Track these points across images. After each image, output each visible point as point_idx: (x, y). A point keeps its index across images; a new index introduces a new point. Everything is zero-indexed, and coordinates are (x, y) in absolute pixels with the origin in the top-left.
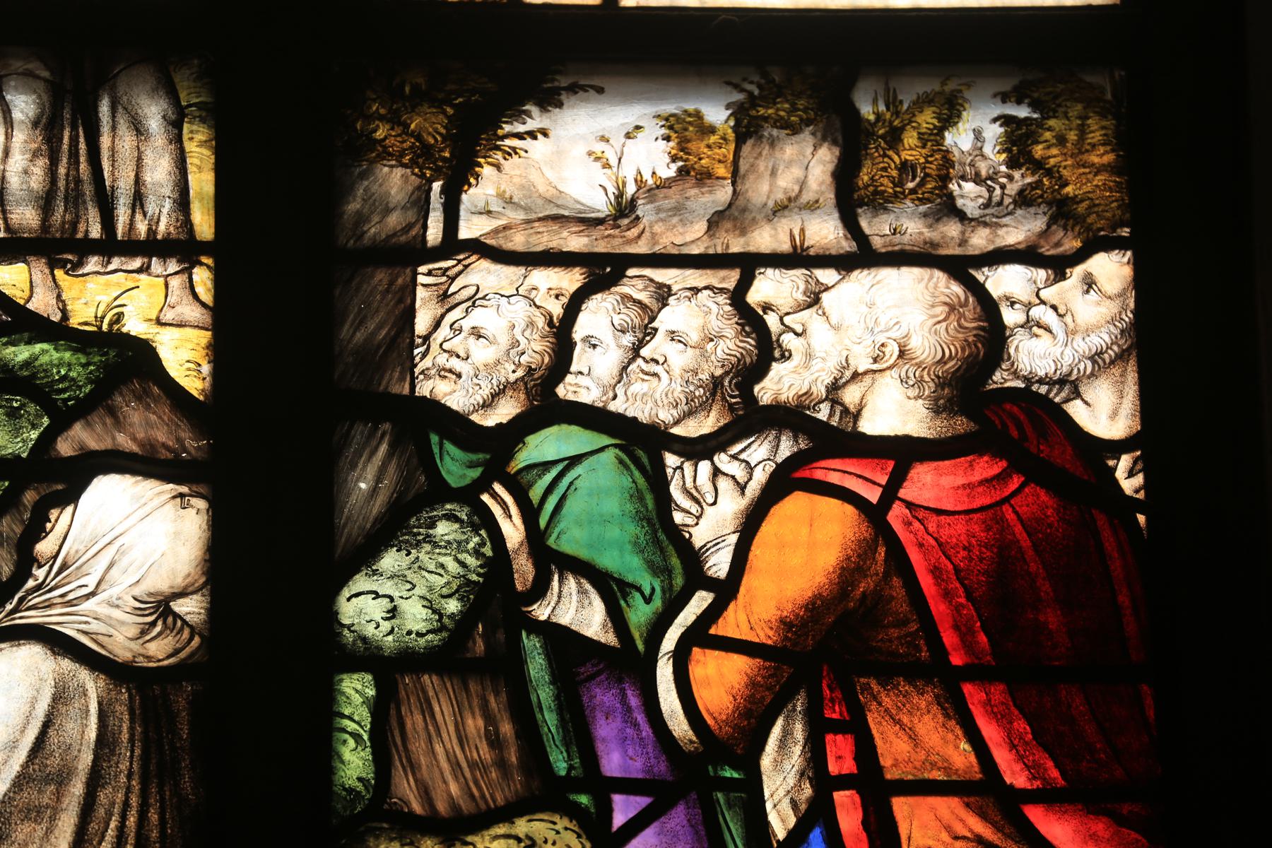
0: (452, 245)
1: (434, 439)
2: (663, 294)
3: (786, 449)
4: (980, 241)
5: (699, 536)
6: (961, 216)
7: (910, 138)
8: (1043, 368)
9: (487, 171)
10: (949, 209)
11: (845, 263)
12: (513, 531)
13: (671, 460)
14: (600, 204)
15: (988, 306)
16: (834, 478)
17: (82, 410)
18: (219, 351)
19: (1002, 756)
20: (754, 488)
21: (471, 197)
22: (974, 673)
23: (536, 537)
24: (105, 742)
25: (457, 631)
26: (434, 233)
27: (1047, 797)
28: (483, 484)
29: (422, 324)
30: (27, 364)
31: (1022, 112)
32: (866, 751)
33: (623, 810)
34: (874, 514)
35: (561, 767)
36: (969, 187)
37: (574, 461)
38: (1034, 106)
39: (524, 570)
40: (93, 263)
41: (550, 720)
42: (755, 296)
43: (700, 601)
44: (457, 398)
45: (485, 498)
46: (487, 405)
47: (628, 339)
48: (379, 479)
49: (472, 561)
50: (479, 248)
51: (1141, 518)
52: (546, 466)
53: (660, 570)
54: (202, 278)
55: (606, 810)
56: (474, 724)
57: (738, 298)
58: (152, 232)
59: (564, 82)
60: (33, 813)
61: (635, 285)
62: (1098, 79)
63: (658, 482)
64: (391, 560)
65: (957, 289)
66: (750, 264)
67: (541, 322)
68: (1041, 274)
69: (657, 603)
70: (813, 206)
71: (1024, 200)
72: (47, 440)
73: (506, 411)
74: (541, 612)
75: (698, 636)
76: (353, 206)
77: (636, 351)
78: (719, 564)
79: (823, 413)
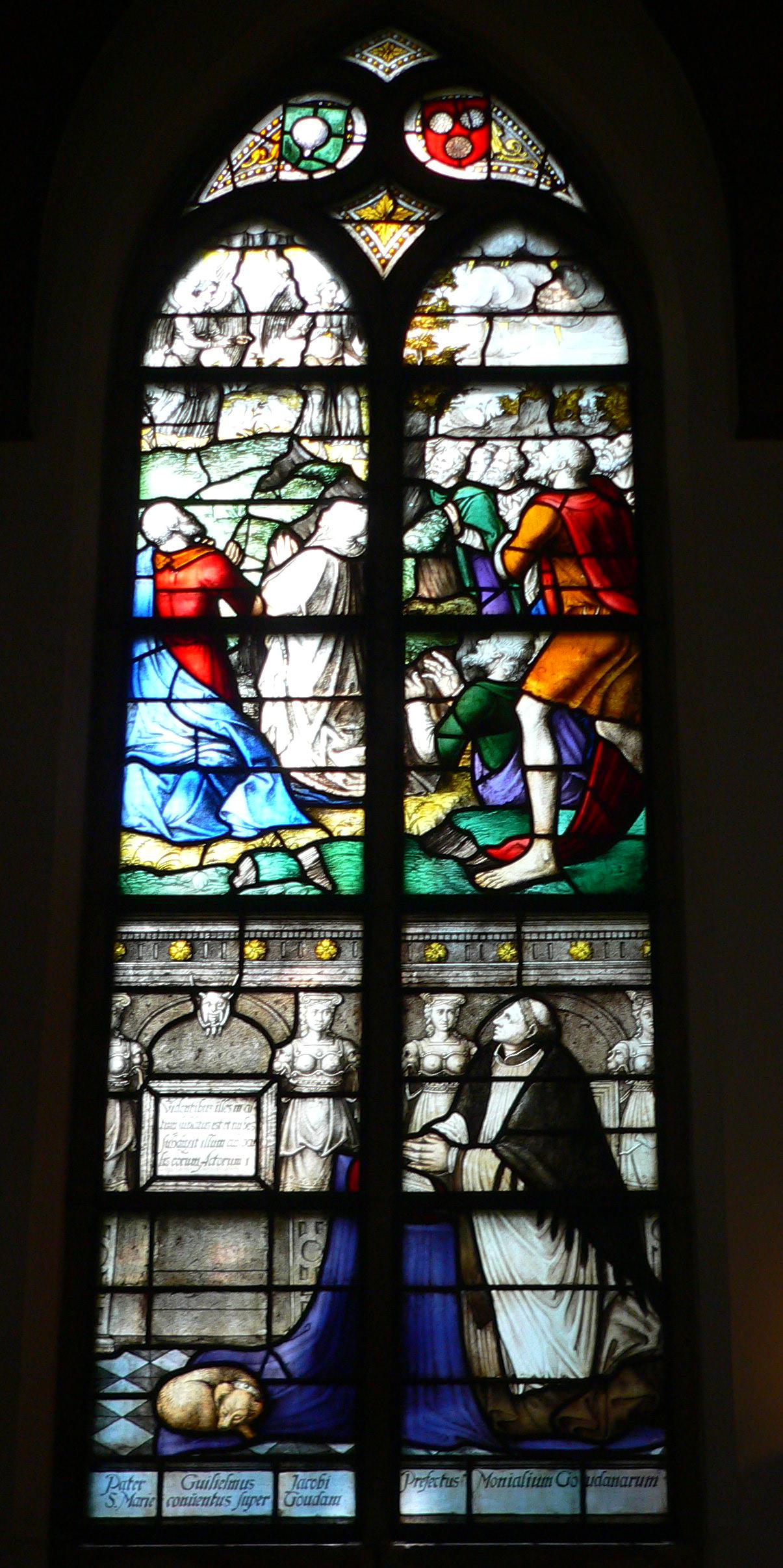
0: (436, 435)
1: (432, 491)
2: (498, 448)
3: (533, 492)
4: (589, 432)
5: (507, 519)
6: (583, 424)
7: (569, 403)
8: (606, 468)
9: (447, 414)
10: (580, 422)
11: (550, 438)
12: (454, 517)
13: (500, 496)
14: (481, 424)
15: (591, 451)
16: (547, 501)
17: (332, 484)
18: (371, 467)
19: (592, 578)
20: (523, 505)
21: (442, 422)
22: (585, 555)
23: (461, 519)
24: (340, 578)
25: (437, 547)
26: (432, 432)
27: (606, 590)
28: (445, 504)
29: (427, 458)
30: (318, 472)
31: (601, 395)
32: (555, 579)
33: (485, 596)
34: (557, 511)
35: (468, 584)
36: (586, 416)
37: (472, 497)
38: (605, 393)
39: (457, 528)
40: (336, 442)
41: (464, 570)
42: (523, 449)
43: (508, 537)
44: (438, 480)
45: (446, 508)
46: (448, 480)
47: (488, 461)
48: (416, 502)
49: (442, 526)
50: (445, 436)
51: (633, 511)
52: (463, 499)
53: (497, 529)
54: (366, 446)
55: (480, 596)
56: (443, 576)
57: (519, 448)
58: (352, 433)
59: (469, 388)
60: (320, 597)
61: (489, 446)
62: (624, 386)
63: (496, 502)
64: (419, 526)
65: (582, 446)
66: (523, 439)
67: (462, 457)
68: (607, 441)
69: (495, 537)
70: (541, 422)
71: (601, 420)
72: (323, 493)
73: (452, 483)
74: (462, 540)
75: (507, 547)
76: (408, 425)
77: (489, 465)
78: (513, 527)
79: (543, 482)
